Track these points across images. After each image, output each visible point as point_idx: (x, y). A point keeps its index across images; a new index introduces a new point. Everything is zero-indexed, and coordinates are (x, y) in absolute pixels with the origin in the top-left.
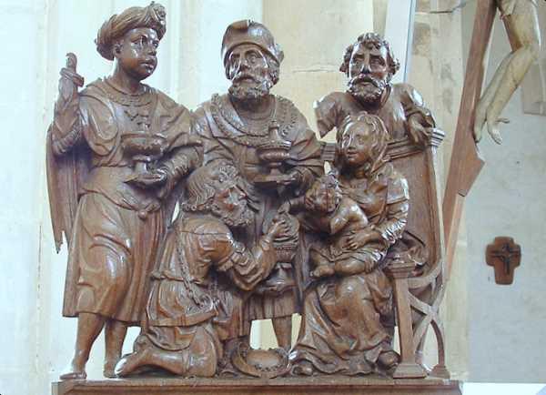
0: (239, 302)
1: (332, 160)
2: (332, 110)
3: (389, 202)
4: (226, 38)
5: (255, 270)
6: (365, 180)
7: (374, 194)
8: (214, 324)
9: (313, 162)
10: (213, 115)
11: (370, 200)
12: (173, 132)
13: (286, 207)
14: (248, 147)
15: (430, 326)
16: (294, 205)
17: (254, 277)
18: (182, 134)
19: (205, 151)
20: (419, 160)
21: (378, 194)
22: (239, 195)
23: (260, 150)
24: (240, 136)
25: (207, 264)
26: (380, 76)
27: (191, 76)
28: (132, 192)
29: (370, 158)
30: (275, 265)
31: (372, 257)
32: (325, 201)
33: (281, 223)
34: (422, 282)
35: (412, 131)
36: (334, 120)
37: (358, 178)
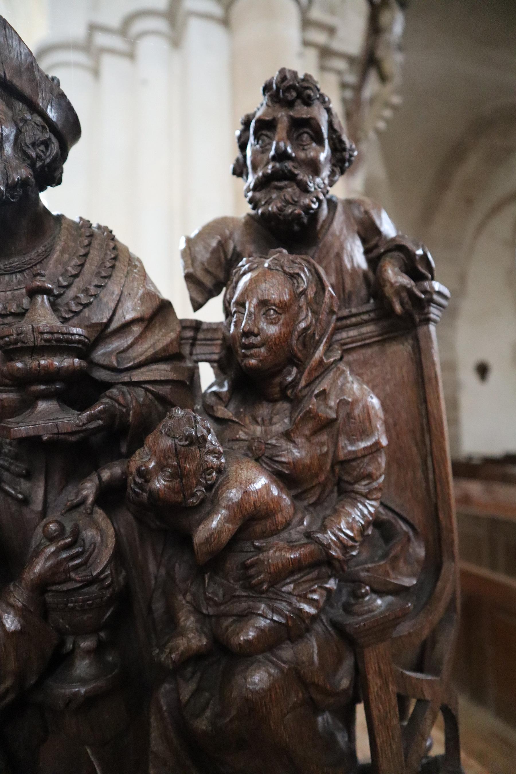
1: (216, 357)
2: (215, 252)
3: (342, 455)
6: (286, 405)
9: (161, 371)
11: (295, 453)
16: (112, 479)
20: (400, 351)
26: (314, 168)
29: (295, 356)
32: (176, 484)
35: (388, 291)
37: (274, 401)
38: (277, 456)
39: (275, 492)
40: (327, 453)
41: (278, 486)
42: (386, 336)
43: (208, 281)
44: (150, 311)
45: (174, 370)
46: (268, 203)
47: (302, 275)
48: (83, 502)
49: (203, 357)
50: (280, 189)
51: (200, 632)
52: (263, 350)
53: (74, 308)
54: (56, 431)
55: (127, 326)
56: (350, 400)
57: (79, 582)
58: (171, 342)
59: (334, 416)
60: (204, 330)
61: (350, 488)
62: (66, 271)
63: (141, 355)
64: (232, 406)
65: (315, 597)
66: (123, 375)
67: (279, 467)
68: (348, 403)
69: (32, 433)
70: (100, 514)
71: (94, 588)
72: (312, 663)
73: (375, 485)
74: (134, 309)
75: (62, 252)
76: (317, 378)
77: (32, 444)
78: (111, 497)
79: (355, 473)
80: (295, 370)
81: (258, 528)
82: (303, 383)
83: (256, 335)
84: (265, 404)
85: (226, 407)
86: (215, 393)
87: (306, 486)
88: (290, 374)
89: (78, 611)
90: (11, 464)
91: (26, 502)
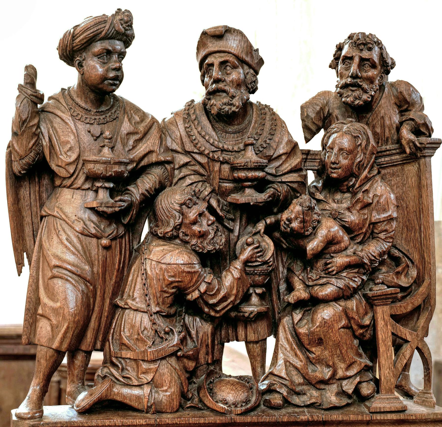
0: (208, 328)
1: (316, 168)
2: (318, 113)
3: (373, 220)
4: (201, 45)
5: (225, 298)
7: (358, 211)
8: (179, 358)
9: (293, 177)
10: (186, 128)
11: (352, 218)
12: (142, 149)
13: (261, 226)
14: (222, 163)
15: (416, 352)
16: (271, 224)
17: (225, 304)
18: (150, 152)
19: (177, 167)
21: (362, 212)
22: (209, 220)
23: (234, 168)
24: (213, 152)
25: (172, 294)
27: (161, 83)
28: (94, 218)
30: (248, 290)
31: (351, 283)
32: (302, 225)
33: (255, 244)
34: (406, 306)
35: (404, 142)
36: (320, 124)
38: (343, 218)
39: (341, 233)
40: (367, 218)
41: (343, 231)
42: (404, 162)
43: (313, 128)
44: (290, 149)
45: (300, 176)
46: (347, 97)
47: (360, 136)
48: (259, 232)
49: (310, 168)
50: (353, 91)
51: (305, 291)
52: (340, 170)
53: (261, 149)
54: (256, 201)
55: (280, 156)
56: (379, 194)
57: (261, 262)
58: (298, 163)
59: (371, 202)
60: (311, 154)
61: (377, 235)
62: (257, 132)
63: (285, 169)
64: (323, 194)
65: (356, 280)
66: (277, 178)
67: (344, 223)
68: (378, 196)
69: (247, 202)
70: (267, 238)
71: (265, 267)
72: (353, 310)
73: (389, 235)
74: (283, 148)
75: (255, 123)
76: (364, 183)
77: (235, 207)
78: (270, 230)
79: (380, 229)
80: (354, 179)
81: (333, 248)
82: (357, 186)
83: (337, 164)
84: (339, 193)
85: (320, 193)
86: (315, 187)
87: (356, 233)
88: (351, 181)
89: (258, 275)
90: (227, 214)
91: (231, 231)
